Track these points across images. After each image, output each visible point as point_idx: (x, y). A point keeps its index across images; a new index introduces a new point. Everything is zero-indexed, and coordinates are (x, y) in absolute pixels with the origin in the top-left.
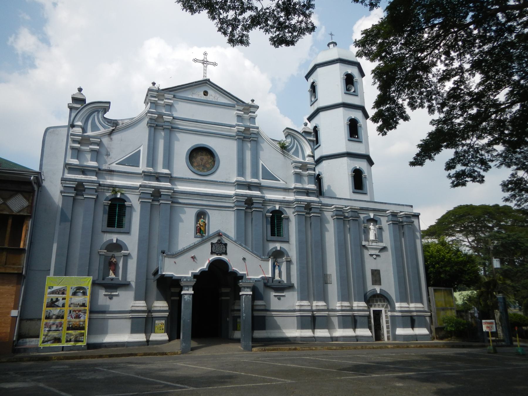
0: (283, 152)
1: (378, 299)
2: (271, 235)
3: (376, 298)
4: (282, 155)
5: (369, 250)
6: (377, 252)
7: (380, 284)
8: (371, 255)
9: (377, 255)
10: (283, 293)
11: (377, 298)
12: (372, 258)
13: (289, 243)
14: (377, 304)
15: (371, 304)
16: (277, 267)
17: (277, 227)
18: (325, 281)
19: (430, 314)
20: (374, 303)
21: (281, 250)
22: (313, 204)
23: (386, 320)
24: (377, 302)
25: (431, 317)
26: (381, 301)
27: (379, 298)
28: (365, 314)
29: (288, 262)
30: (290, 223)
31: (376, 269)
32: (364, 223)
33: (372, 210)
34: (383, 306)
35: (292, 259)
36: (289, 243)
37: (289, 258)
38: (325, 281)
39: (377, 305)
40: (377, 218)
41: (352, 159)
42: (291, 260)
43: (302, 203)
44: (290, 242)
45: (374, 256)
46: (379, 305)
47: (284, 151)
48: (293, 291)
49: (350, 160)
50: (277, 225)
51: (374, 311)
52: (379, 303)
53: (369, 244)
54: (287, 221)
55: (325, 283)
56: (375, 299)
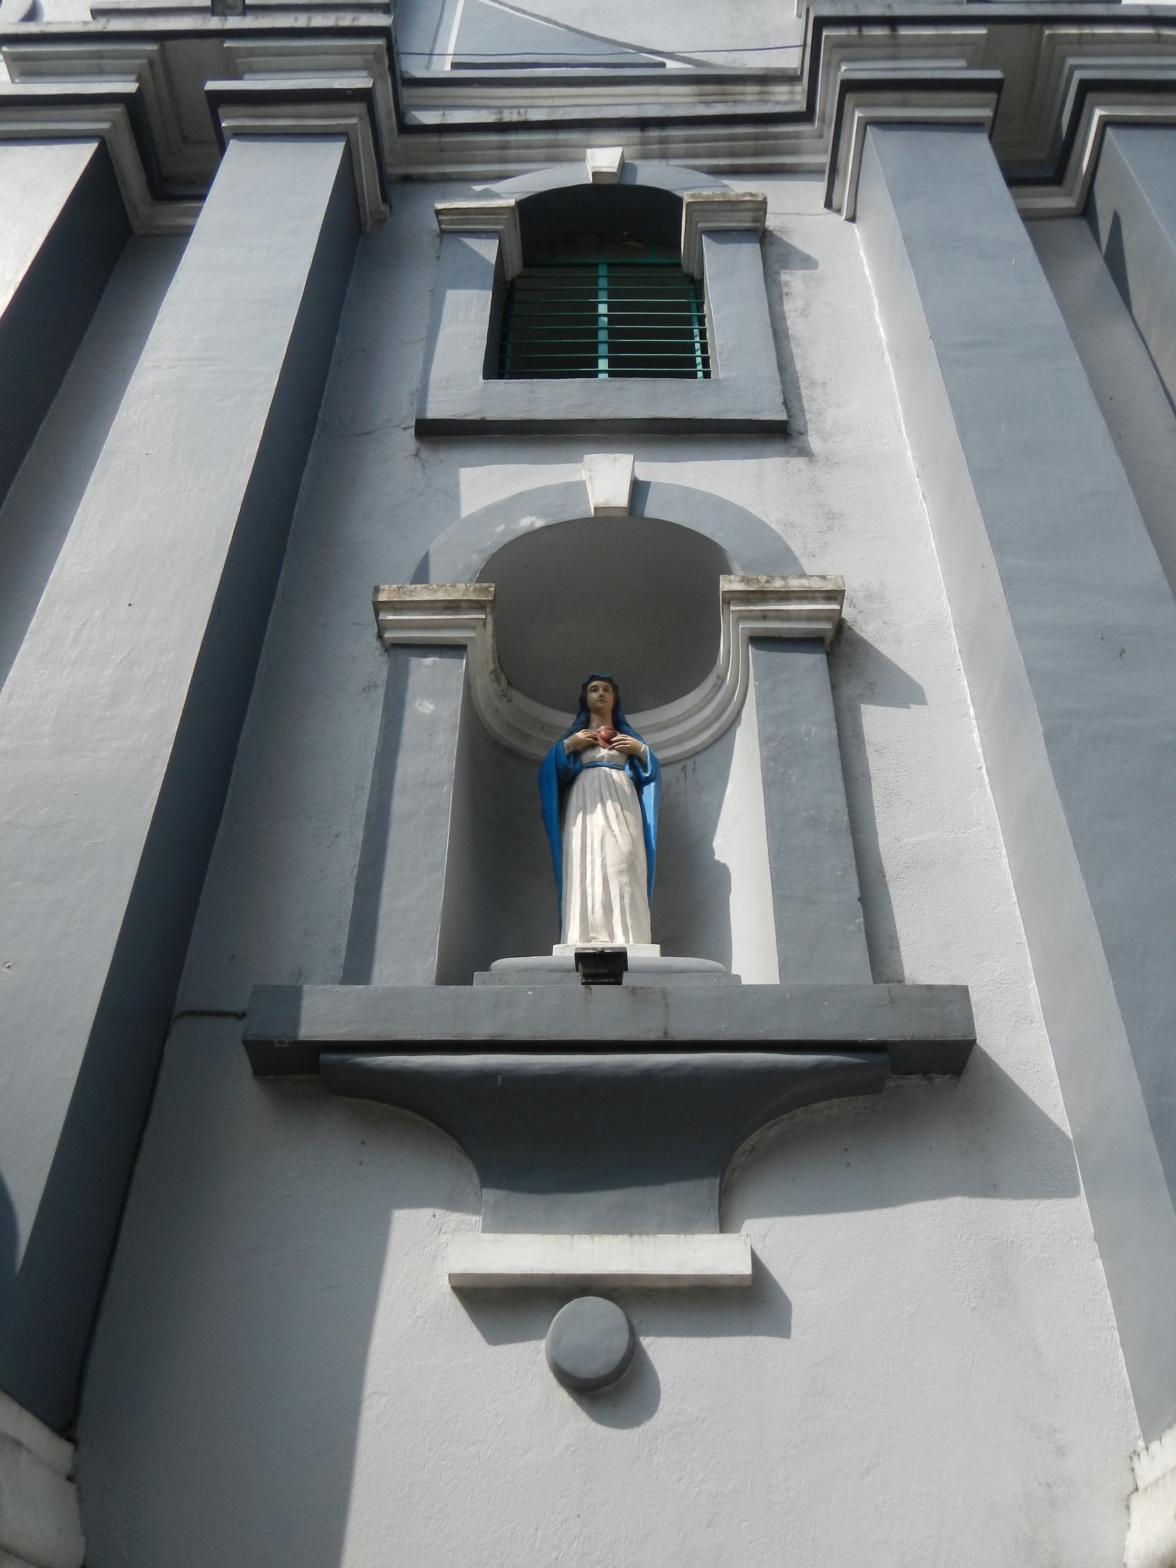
2: (487, 376)
10: (725, 1223)
13: (805, 452)
16: (621, 777)
17: (612, 347)
21: (653, 509)
22: (1073, 31)
29: (812, 663)
30: (793, 280)
35: (868, 629)
36: (805, 452)
37: (795, 584)
42: (841, 627)
44: (814, 442)
48: (989, 1189)
50: (612, 333)
54: (749, 252)
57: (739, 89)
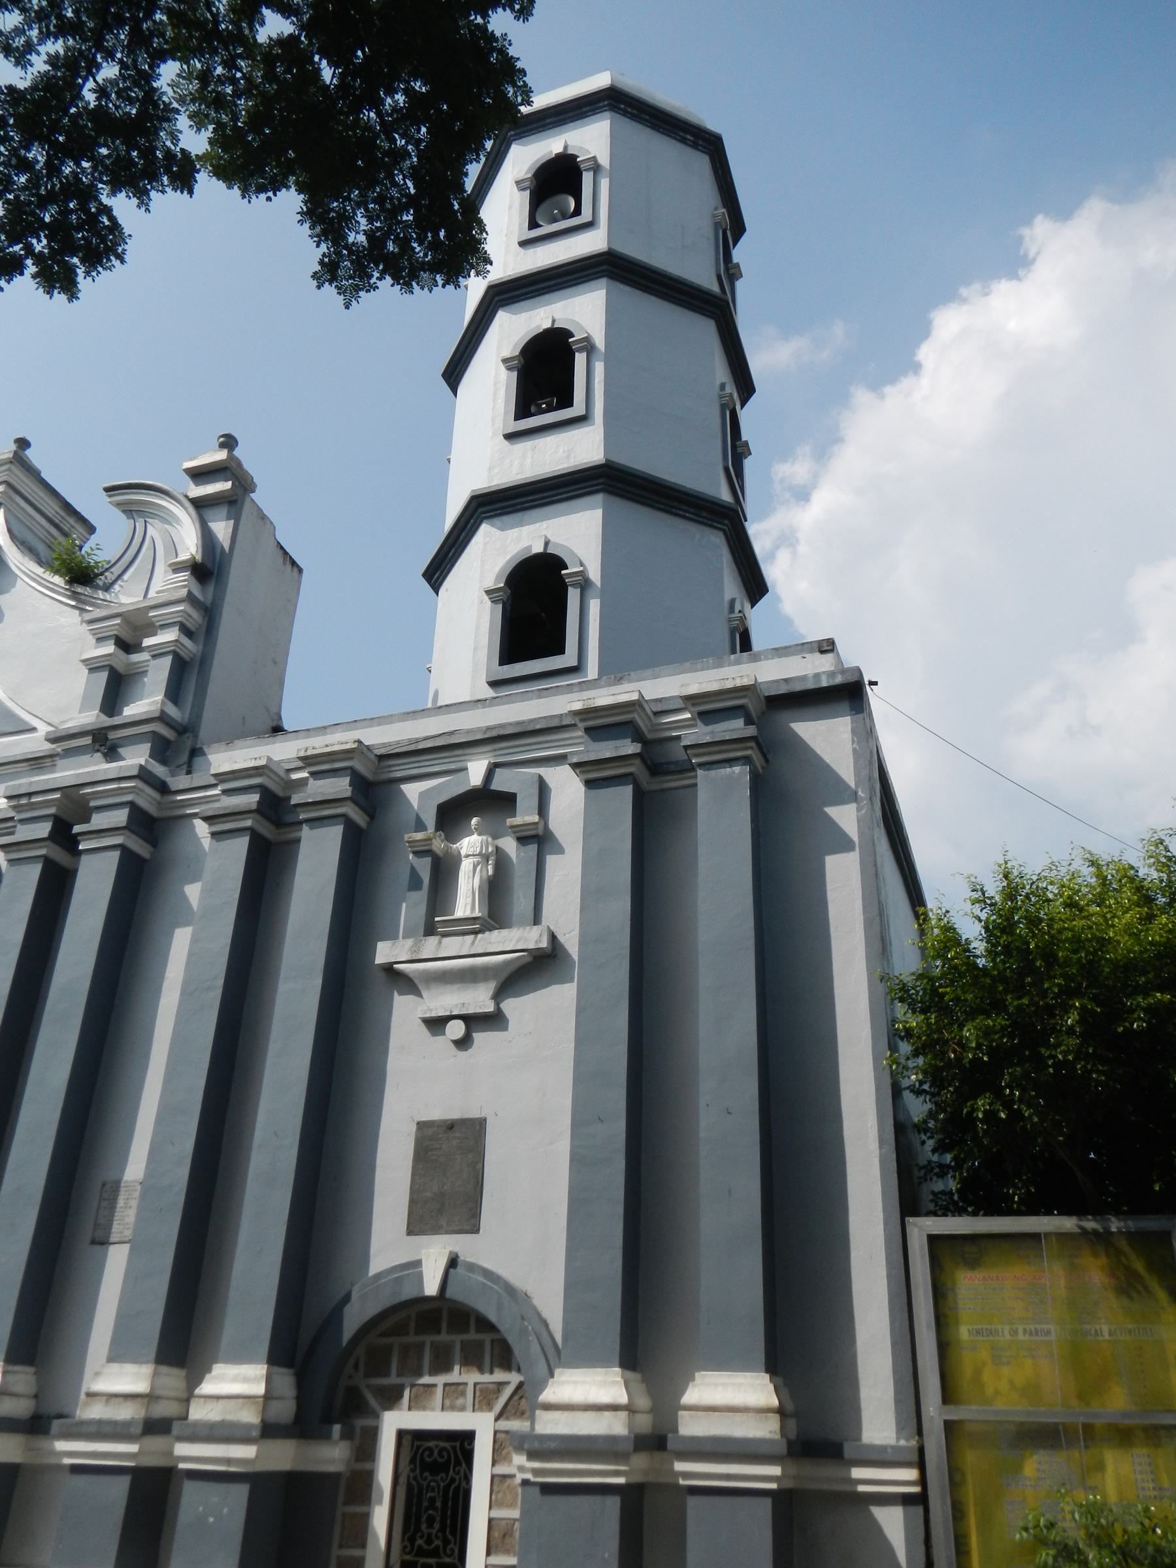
0: (74, 596)
1: (457, 1339)
3: (439, 1332)
4: (77, 612)
5: (425, 994)
6: (479, 999)
7: (471, 1223)
8: (436, 1024)
9: (474, 1022)
11: (443, 1337)
12: (440, 1039)
14: (440, 1380)
15: (393, 1380)
18: (96, 1226)
19: (912, 1474)
20: (420, 1375)
23: (490, 1521)
24: (442, 1365)
25: (917, 1501)
26: (472, 1359)
27: (466, 1330)
28: (228, 1461)
31: (455, 1115)
32: (420, 826)
33: (479, 736)
34: (484, 1398)
38: (96, 1226)
39: (439, 1391)
40: (503, 782)
41: (507, 519)
43: (34, 799)
45: (456, 1029)
46: (454, 1390)
47: (80, 589)
49: (502, 529)
51: (465, 1439)
52: (456, 1375)
53: (417, 951)
55: (93, 1242)
56: (428, 1339)
57: (43, 761)
